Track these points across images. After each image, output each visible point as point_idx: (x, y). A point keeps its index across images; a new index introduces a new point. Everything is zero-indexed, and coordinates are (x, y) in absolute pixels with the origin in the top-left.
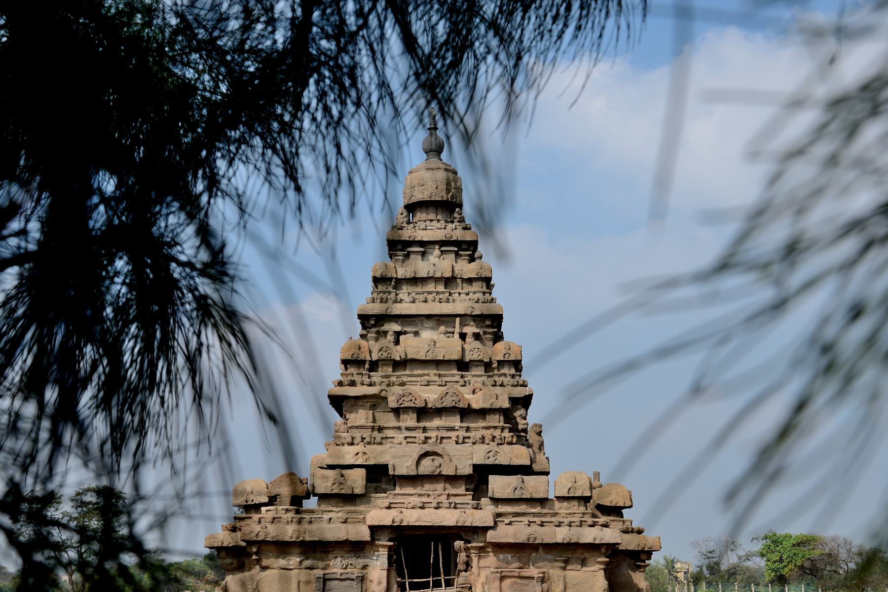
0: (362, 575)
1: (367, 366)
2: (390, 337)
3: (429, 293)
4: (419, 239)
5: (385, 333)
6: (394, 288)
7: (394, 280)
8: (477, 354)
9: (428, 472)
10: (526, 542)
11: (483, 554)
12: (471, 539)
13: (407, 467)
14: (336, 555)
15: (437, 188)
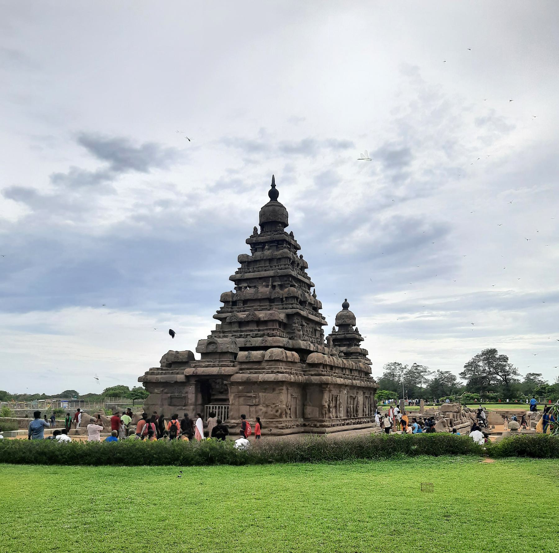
7: (247, 262)
10: (246, 381)
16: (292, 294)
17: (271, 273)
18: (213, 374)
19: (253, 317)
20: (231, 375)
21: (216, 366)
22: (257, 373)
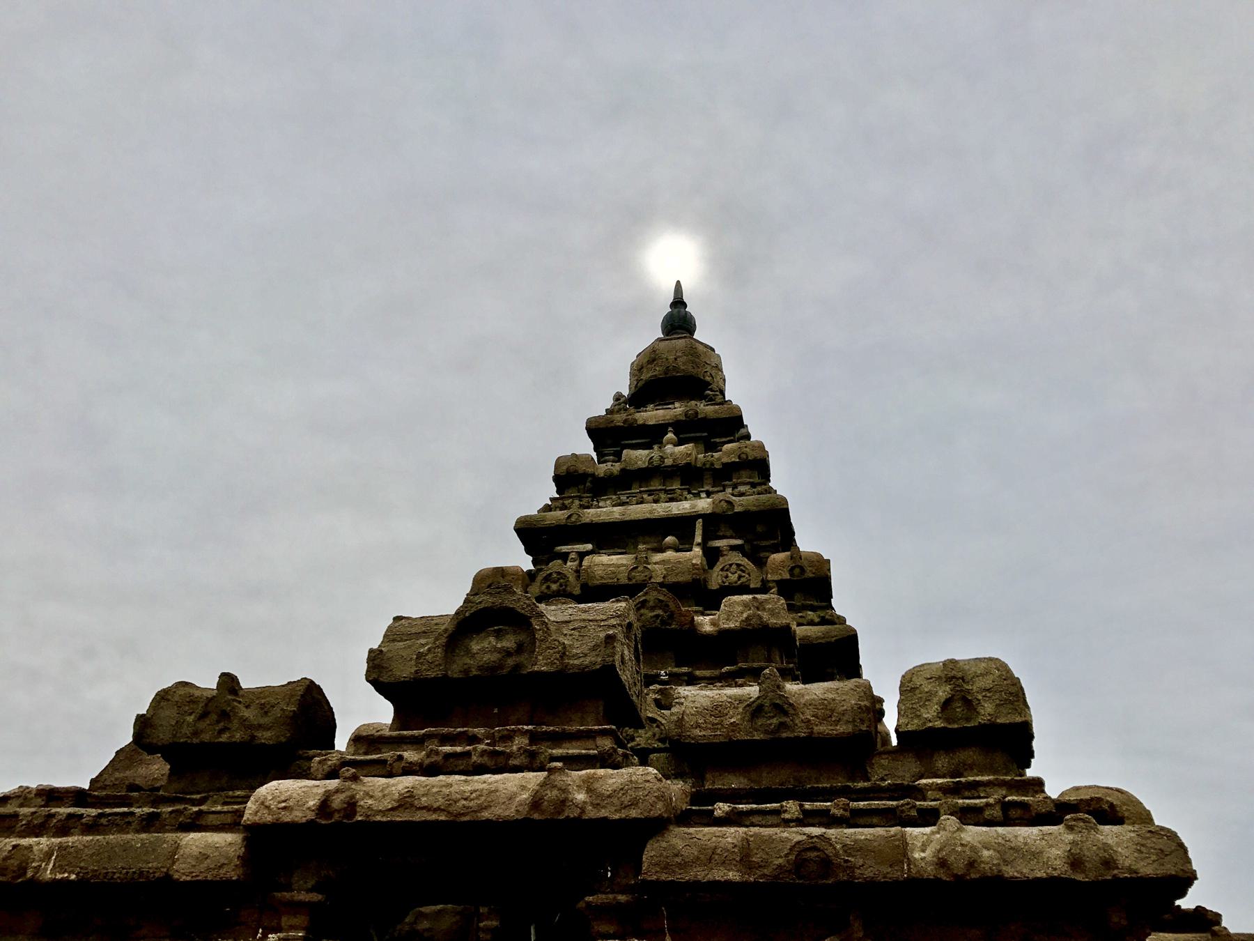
3: (650, 493)
5: (564, 557)
8: (736, 575)
9: (480, 668)
17: (703, 504)
19: (660, 612)
21: (512, 762)
22: (861, 821)
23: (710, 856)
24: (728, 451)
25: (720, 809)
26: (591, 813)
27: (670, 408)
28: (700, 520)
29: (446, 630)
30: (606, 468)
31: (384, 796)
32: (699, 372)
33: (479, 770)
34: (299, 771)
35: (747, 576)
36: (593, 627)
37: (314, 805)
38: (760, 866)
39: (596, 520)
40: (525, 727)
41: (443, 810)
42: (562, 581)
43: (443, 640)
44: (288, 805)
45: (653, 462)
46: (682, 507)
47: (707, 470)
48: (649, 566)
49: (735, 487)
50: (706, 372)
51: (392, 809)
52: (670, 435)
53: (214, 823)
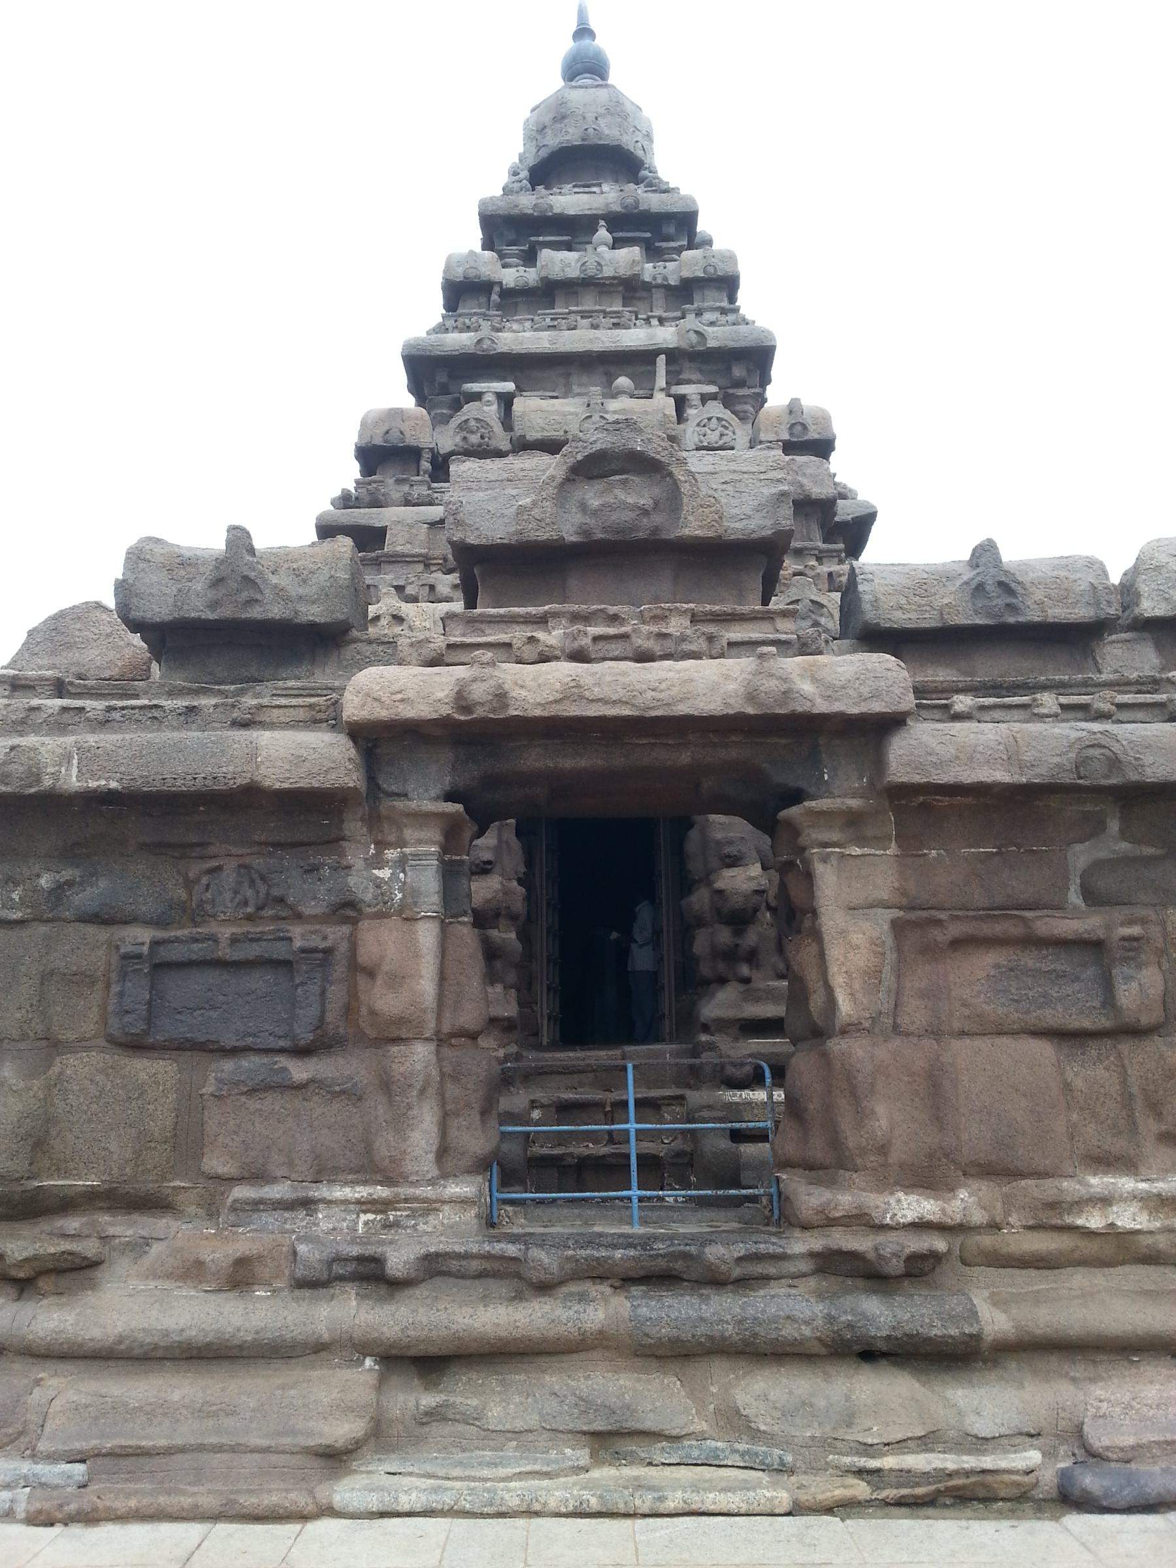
0: (323, 945)
1: (426, 465)
2: (490, 411)
3: (585, 315)
4: (557, 210)
5: (477, 396)
6: (499, 307)
7: (497, 289)
8: (717, 433)
9: (605, 529)
11: (856, 851)
12: (802, 784)
13: (522, 510)
14: (214, 863)
15: (596, 118)
16: (811, 428)
17: (665, 336)
18: (682, 709)
20: (893, 722)
21: (686, 647)
23: (969, 756)
24: (689, 263)
25: (961, 702)
26: (822, 707)
27: (595, 193)
28: (663, 357)
29: (553, 478)
30: (518, 274)
31: (539, 686)
32: (628, 141)
33: (643, 657)
34: (359, 657)
35: (731, 434)
36: (751, 481)
37: (447, 696)
38: (1033, 766)
39: (517, 348)
40: (685, 606)
41: (627, 703)
42: (483, 430)
43: (551, 491)
44: (406, 697)
45: (585, 270)
46: (635, 337)
47: (658, 286)
48: (605, 416)
49: (699, 313)
50: (637, 142)
51: (556, 701)
52: (603, 233)
53: (282, 719)
